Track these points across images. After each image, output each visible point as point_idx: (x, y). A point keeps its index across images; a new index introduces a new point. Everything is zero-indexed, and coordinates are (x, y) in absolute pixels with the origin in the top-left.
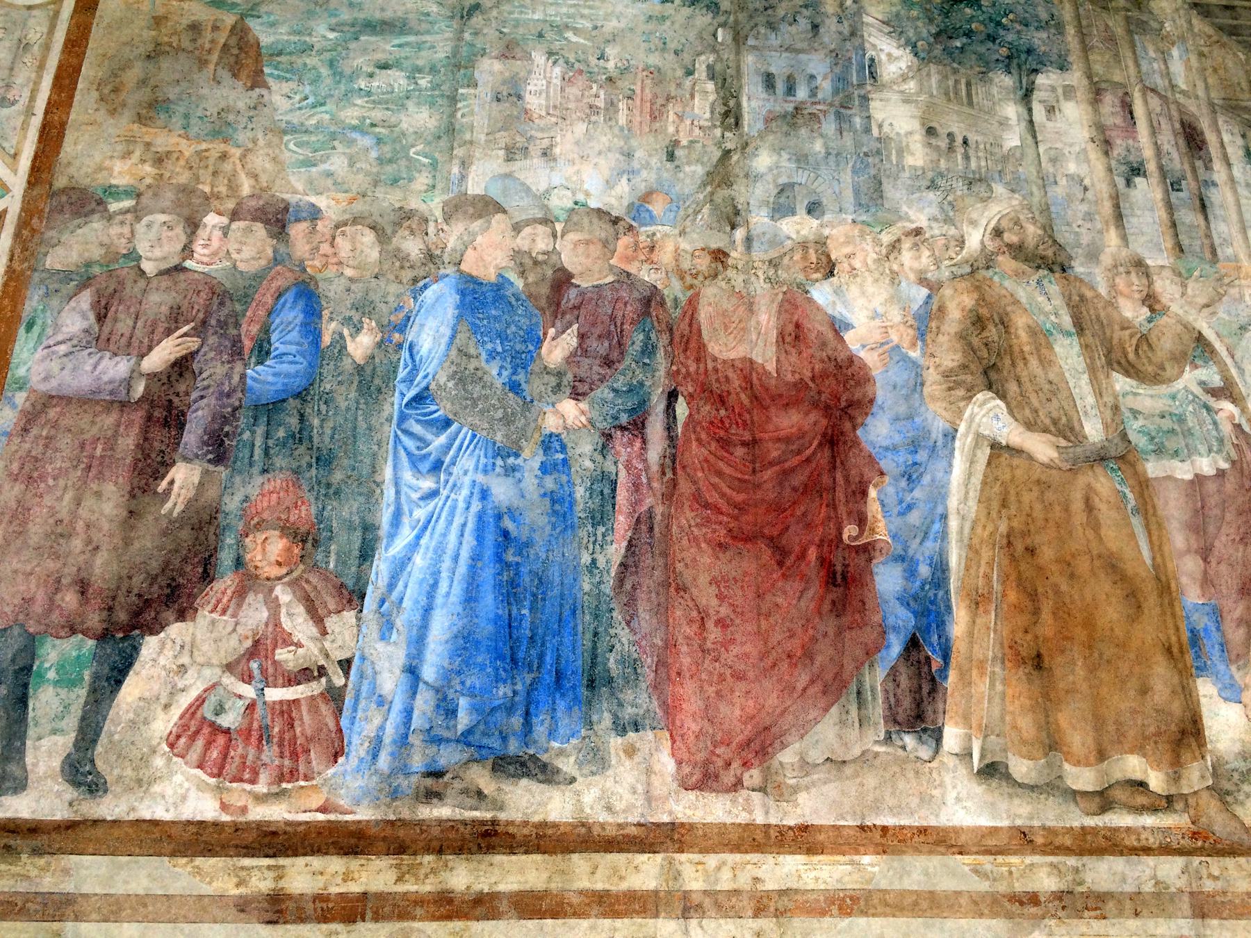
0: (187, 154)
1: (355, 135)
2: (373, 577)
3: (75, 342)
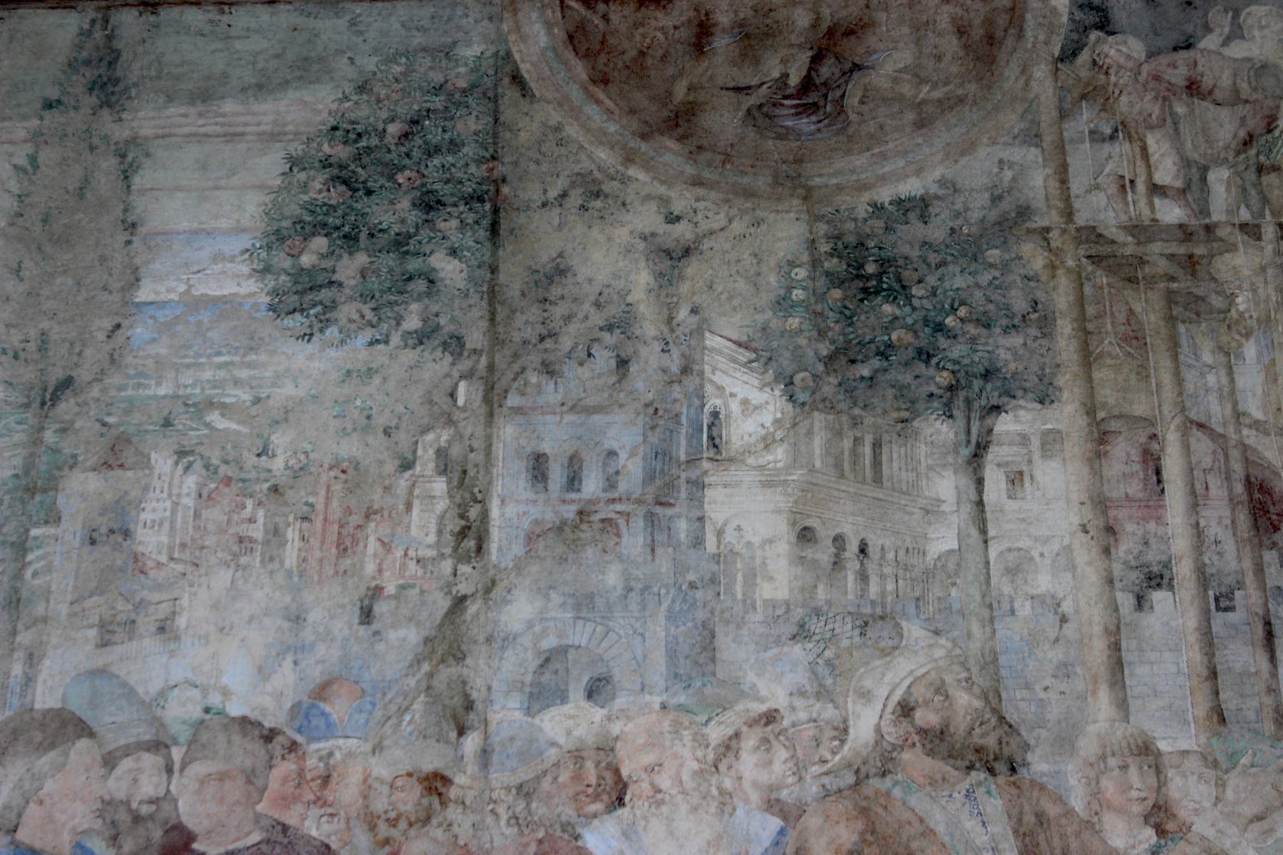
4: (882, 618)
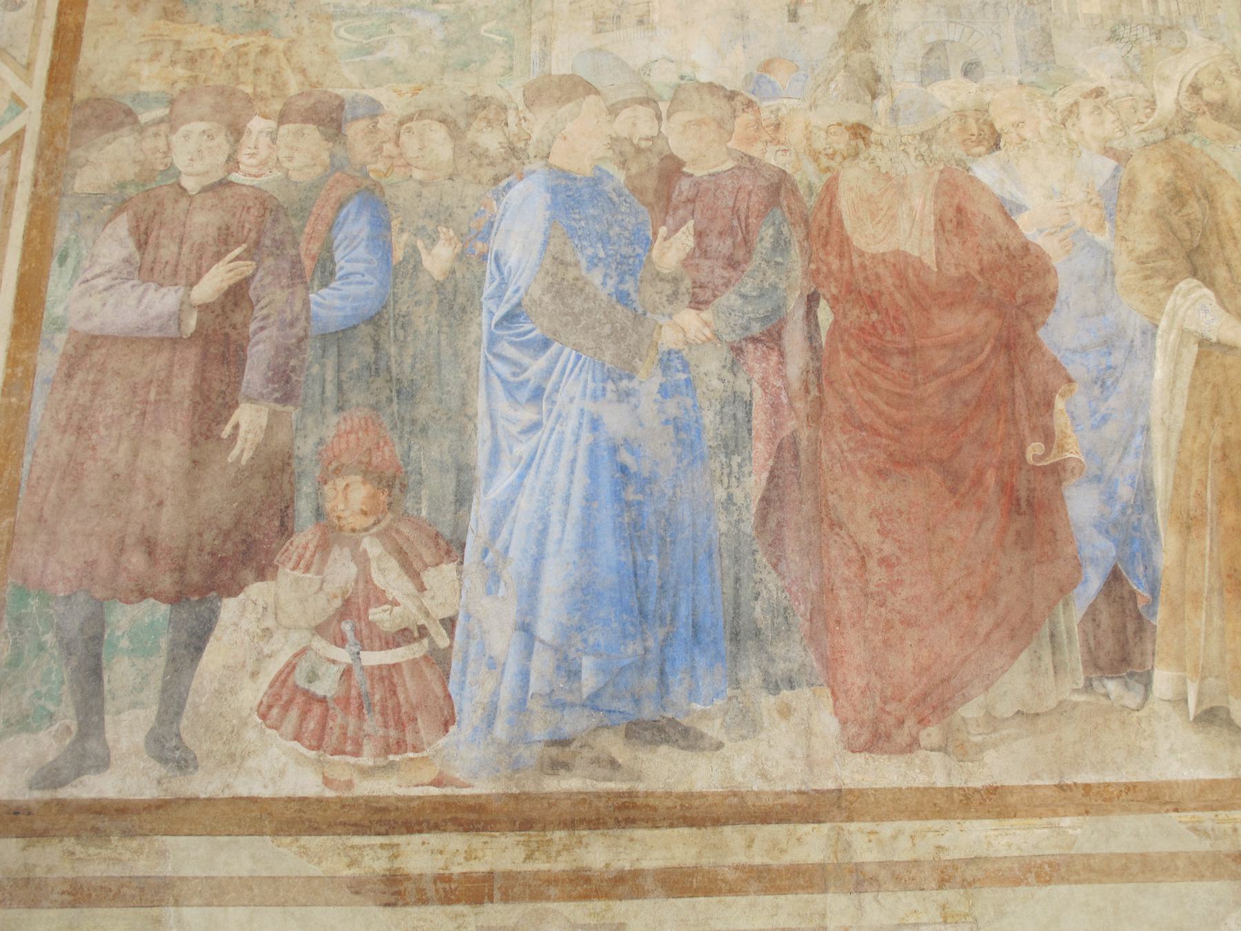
0: (222, 50)
1: (414, 15)
2: (472, 524)
3: (115, 274)
4: (1170, 28)
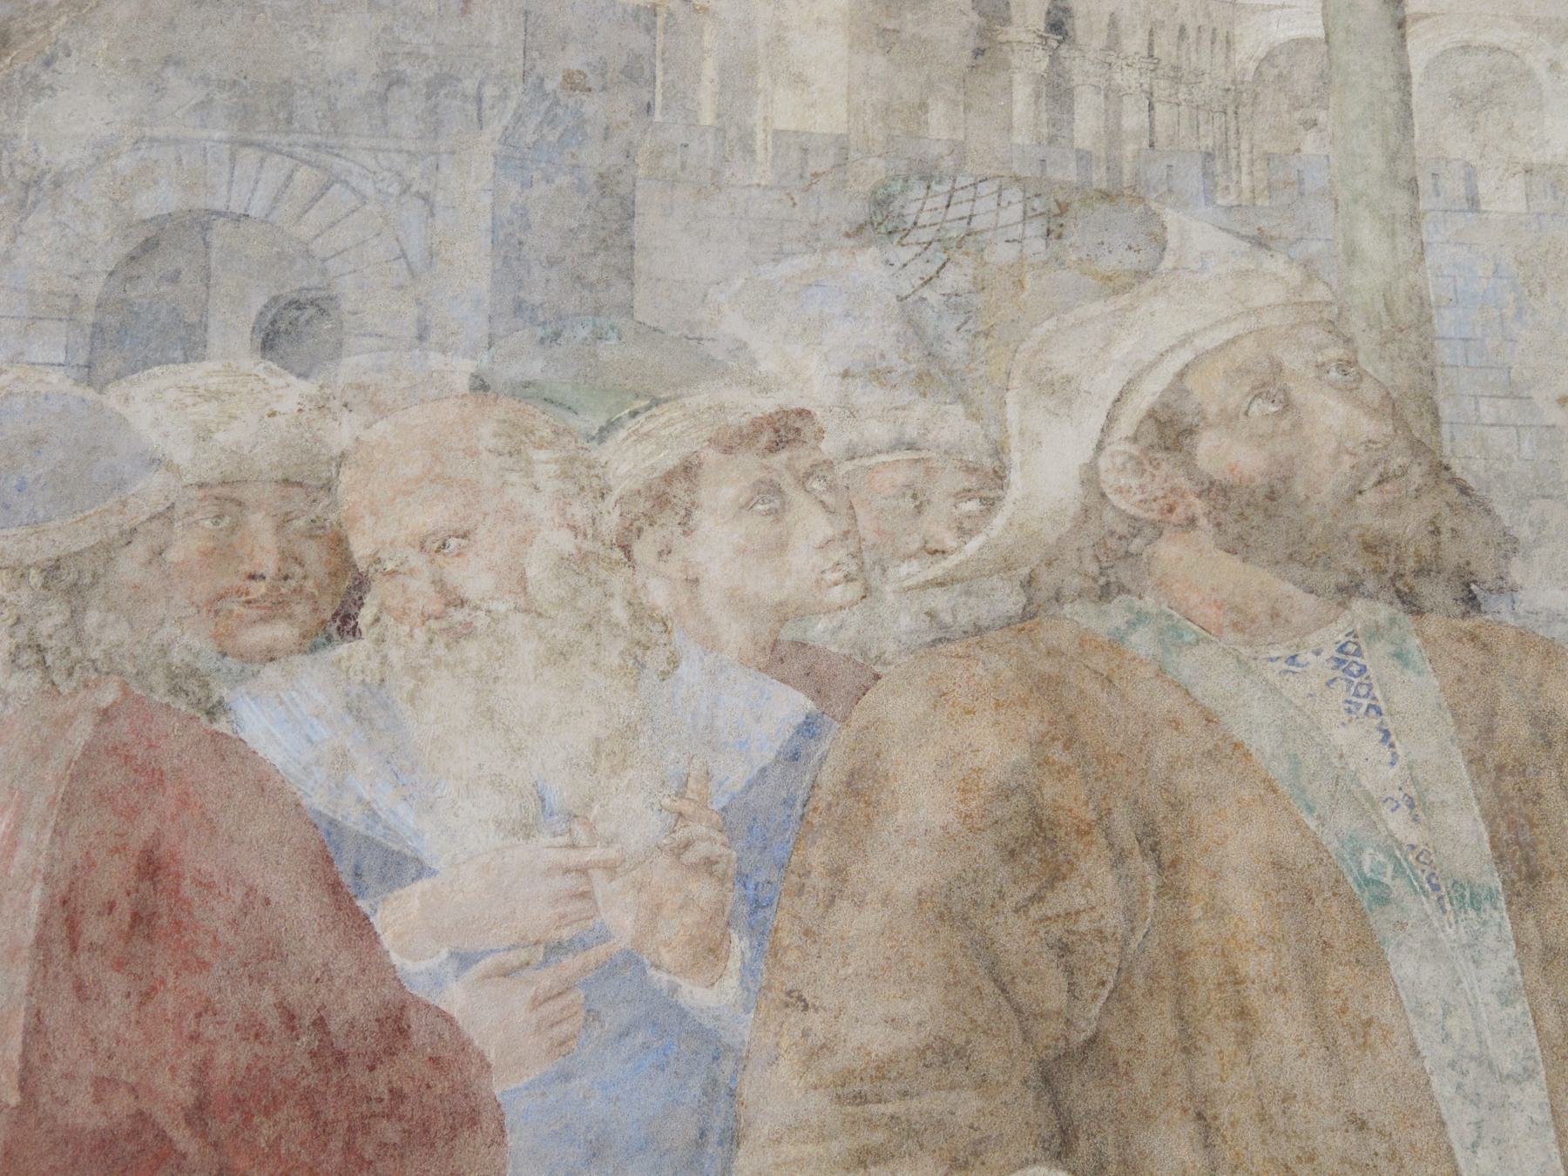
4: (1106, 196)
